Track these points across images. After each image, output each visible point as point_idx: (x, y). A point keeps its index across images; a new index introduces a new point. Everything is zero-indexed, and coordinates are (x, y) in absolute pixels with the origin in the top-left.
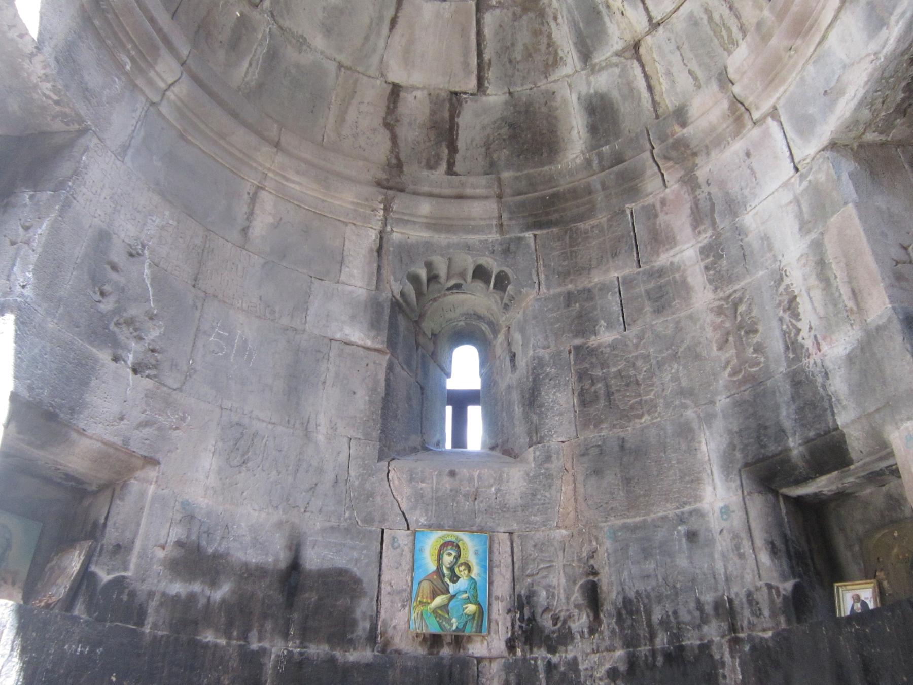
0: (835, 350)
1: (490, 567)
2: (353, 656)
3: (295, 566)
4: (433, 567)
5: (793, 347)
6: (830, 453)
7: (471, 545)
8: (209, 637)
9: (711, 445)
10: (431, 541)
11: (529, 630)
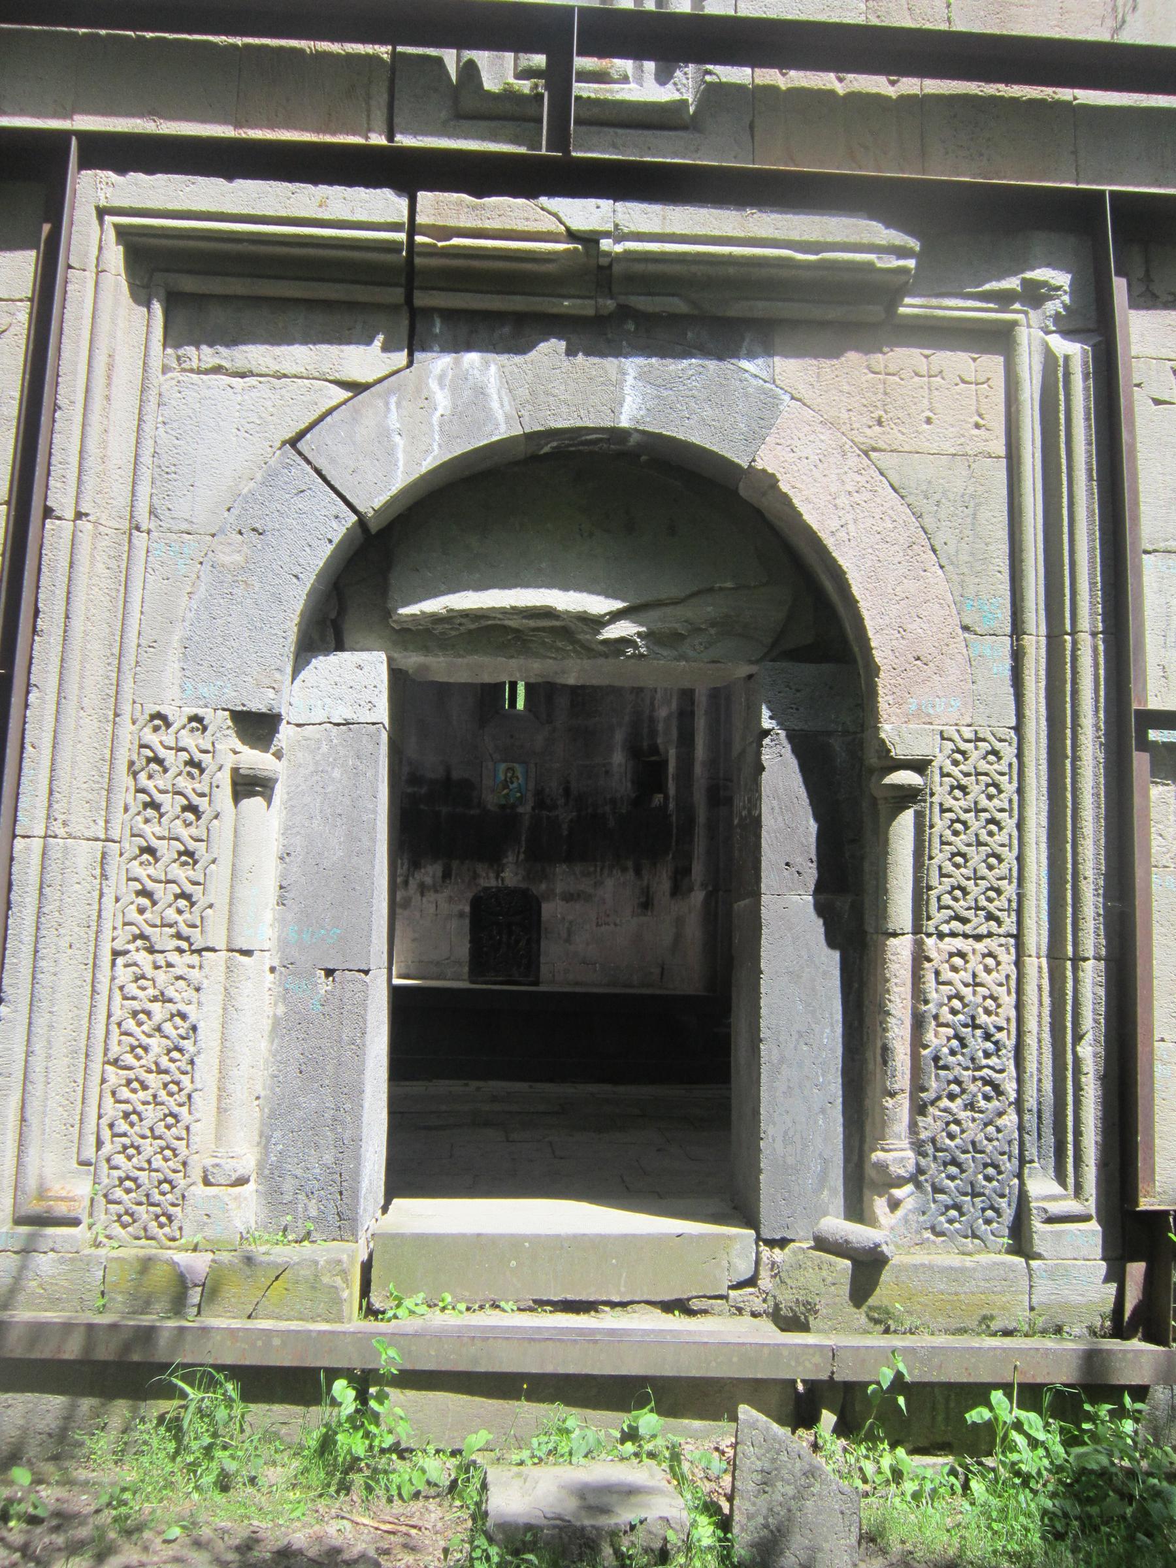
0: (662, 713)
1: (527, 778)
2: (472, 812)
3: (448, 778)
4: (503, 778)
5: (652, 704)
6: (654, 749)
7: (519, 769)
8: (422, 807)
9: (619, 736)
10: (502, 767)
11: (542, 801)
